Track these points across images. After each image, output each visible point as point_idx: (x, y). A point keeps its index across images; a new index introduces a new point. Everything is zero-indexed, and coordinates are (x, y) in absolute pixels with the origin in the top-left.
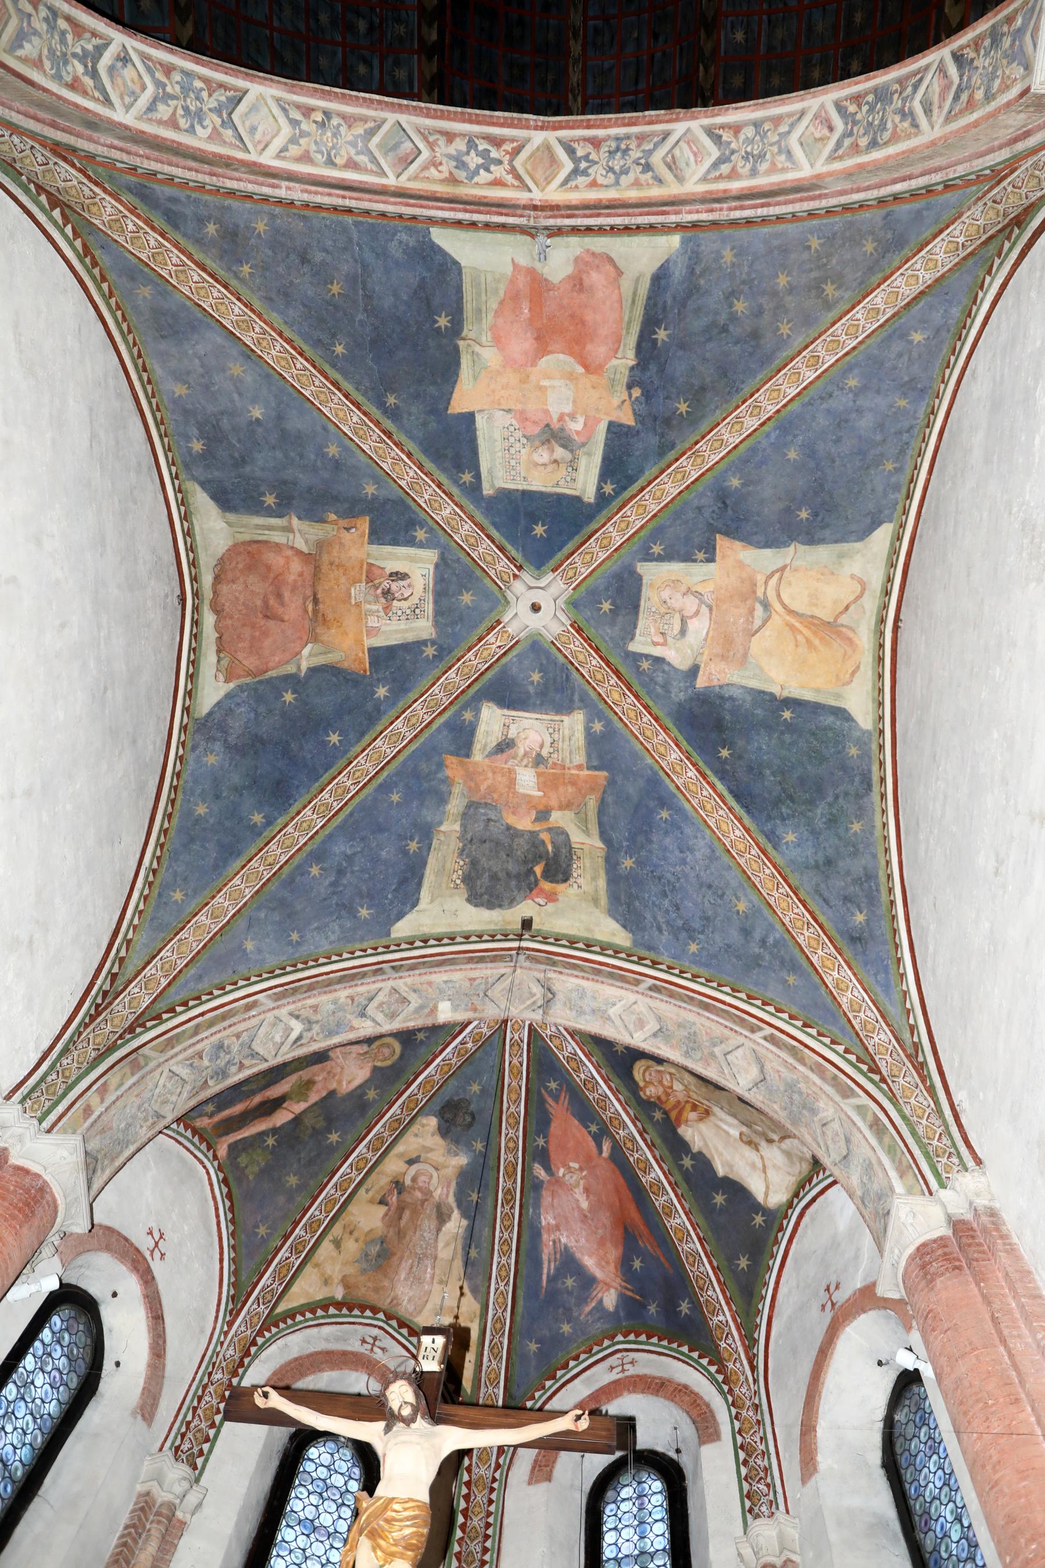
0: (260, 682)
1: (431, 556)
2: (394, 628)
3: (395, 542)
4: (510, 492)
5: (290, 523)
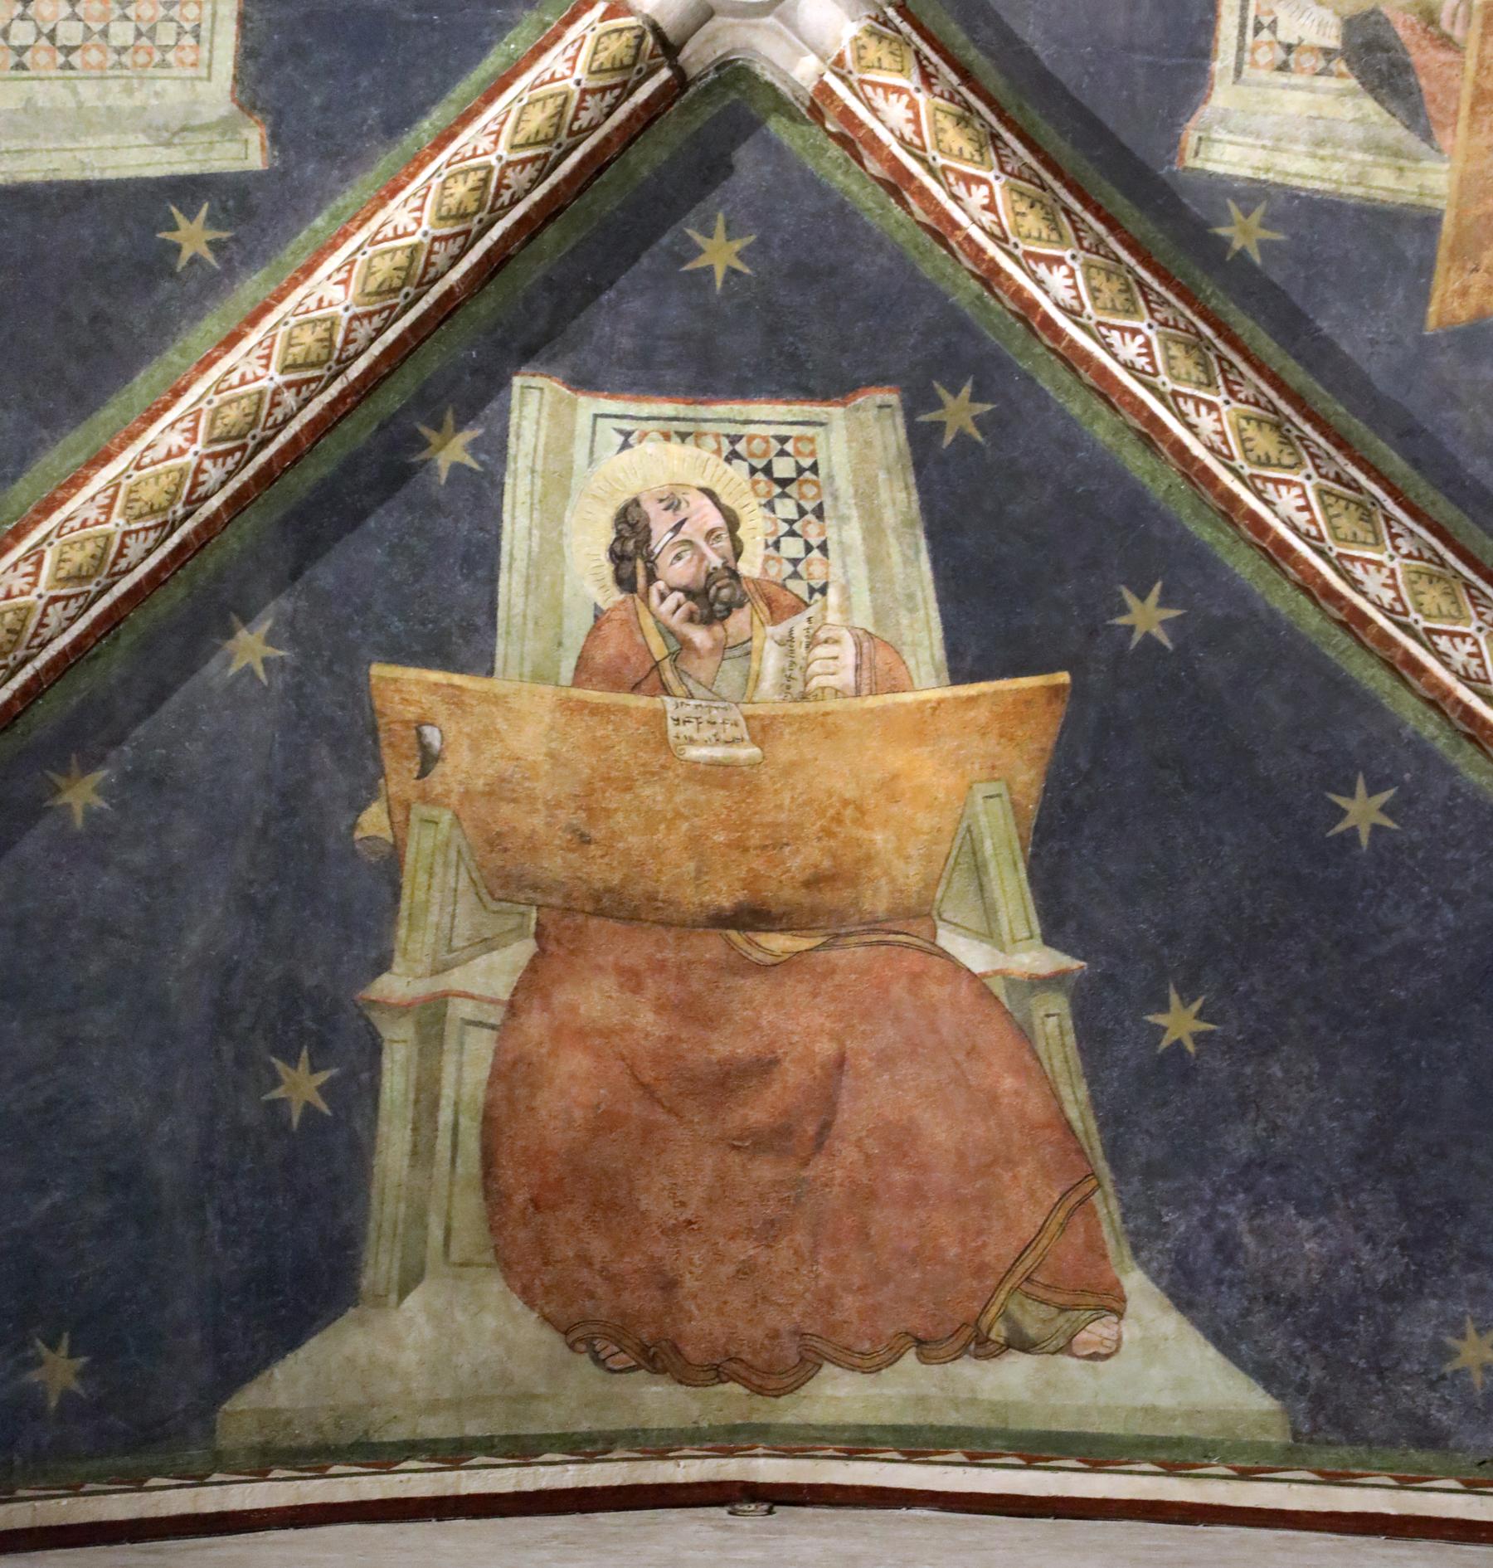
0: (1116, 1154)
1: (535, 404)
2: (859, 572)
3: (483, 559)
4: (247, 53)
5: (403, 1009)
